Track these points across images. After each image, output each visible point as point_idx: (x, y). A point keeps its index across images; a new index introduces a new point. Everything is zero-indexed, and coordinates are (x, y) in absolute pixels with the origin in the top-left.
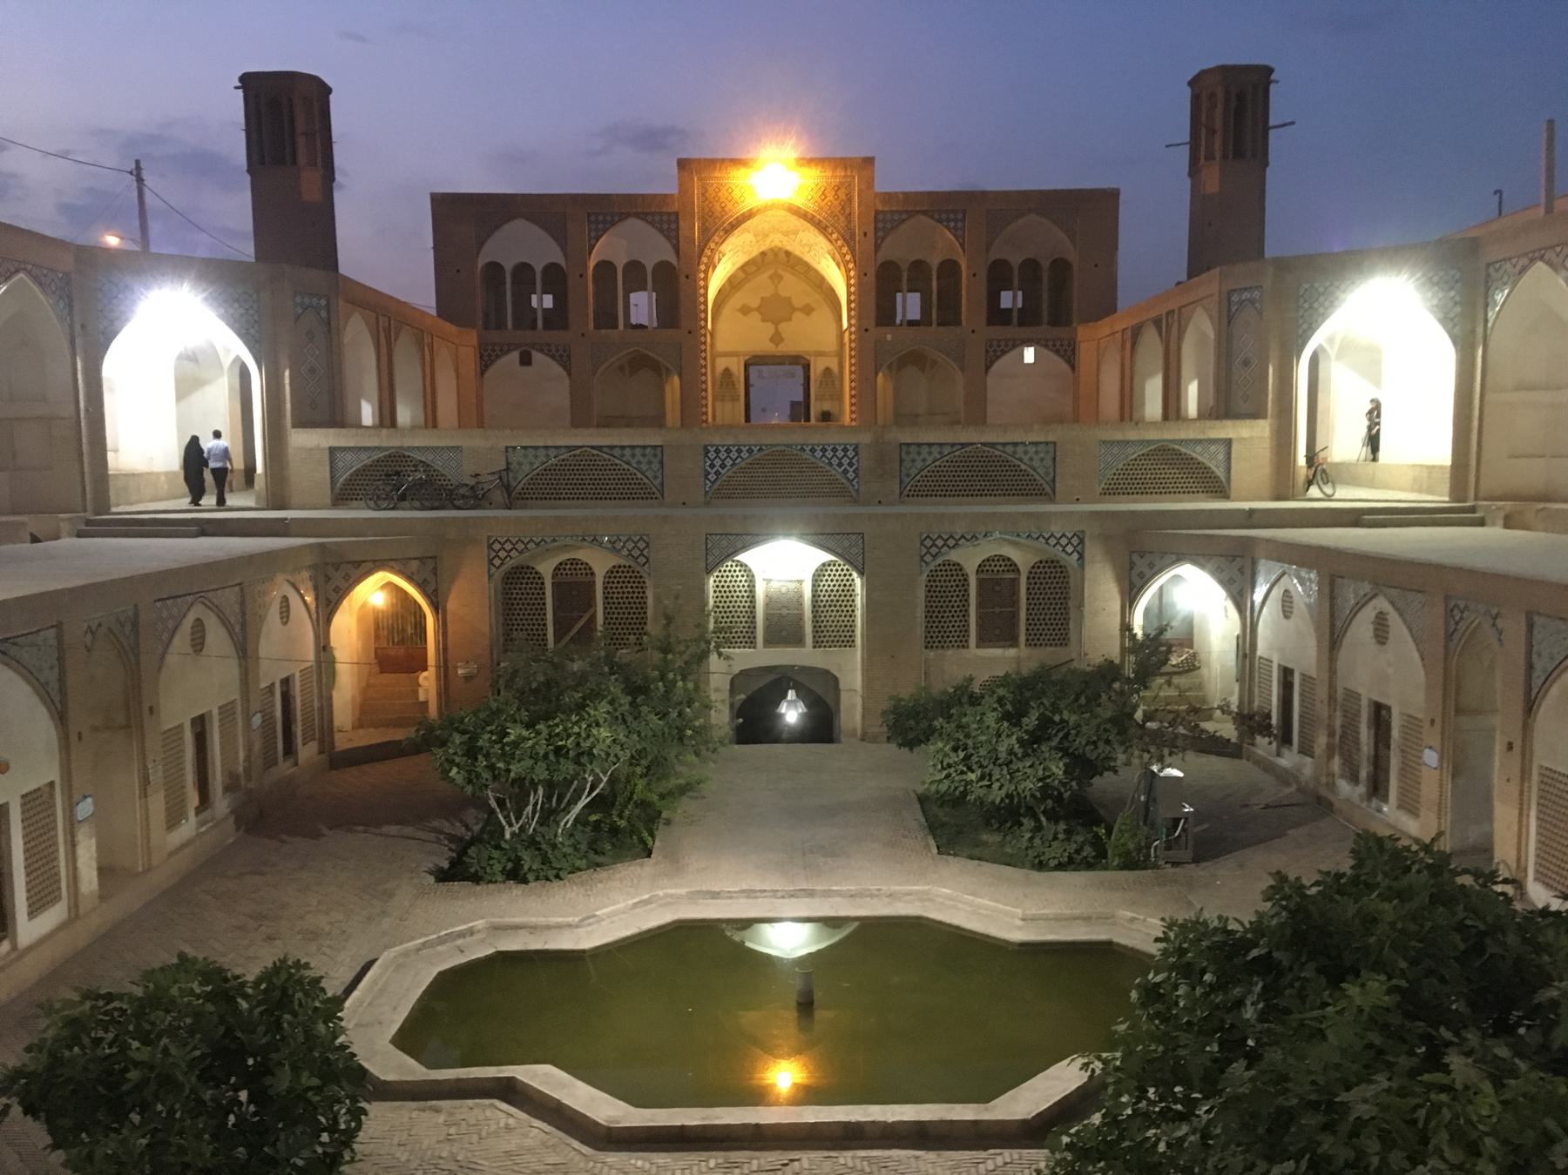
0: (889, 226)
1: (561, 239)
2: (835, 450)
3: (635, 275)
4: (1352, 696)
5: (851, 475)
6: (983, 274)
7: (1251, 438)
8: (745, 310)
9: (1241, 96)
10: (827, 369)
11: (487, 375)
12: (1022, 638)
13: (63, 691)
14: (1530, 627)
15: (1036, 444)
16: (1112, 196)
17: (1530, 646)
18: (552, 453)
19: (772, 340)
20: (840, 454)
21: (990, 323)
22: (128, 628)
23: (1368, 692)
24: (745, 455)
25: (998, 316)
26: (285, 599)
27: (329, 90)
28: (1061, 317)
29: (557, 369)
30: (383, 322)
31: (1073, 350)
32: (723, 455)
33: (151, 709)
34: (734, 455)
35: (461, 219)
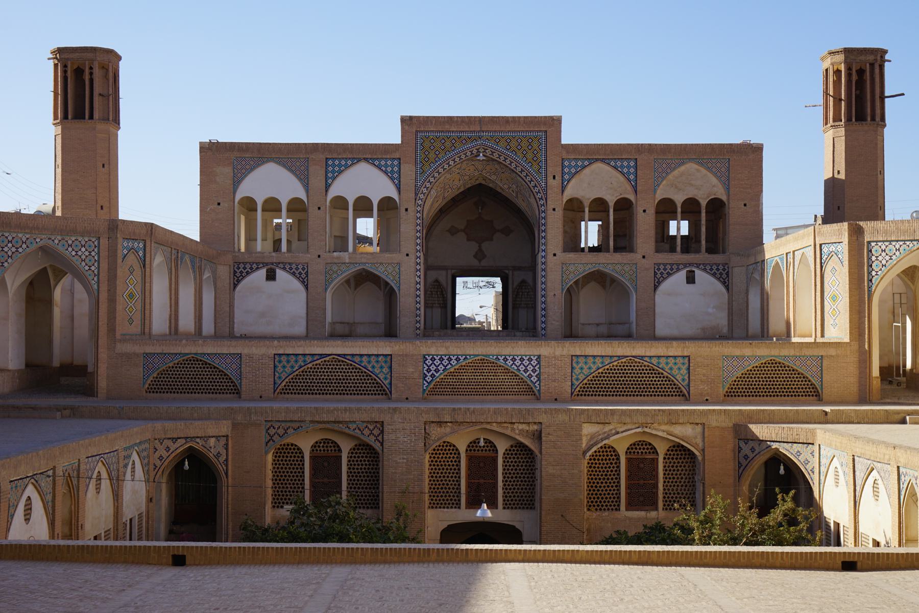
0: (573, 170)
1: (305, 181)
2: (522, 360)
3: (363, 207)
5: (534, 379)
6: (651, 211)
7: (838, 356)
8: (453, 231)
9: (861, 72)
10: (523, 281)
11: (238, 289)
12: (660, 504)
13: (54, 511)
15: (675, 357)
16: (757, 150)
18: (309, 359)
19: (475, 256)
20: (526, 362)
21: (658, 251)
24: (454, 362)
25: (665, 241)
26: (134, 464)
27: (120, 58)
29: (296, 284)
31: (727, 274)
32: (437, 362)
34: (445, 362)
35: (224, 163)
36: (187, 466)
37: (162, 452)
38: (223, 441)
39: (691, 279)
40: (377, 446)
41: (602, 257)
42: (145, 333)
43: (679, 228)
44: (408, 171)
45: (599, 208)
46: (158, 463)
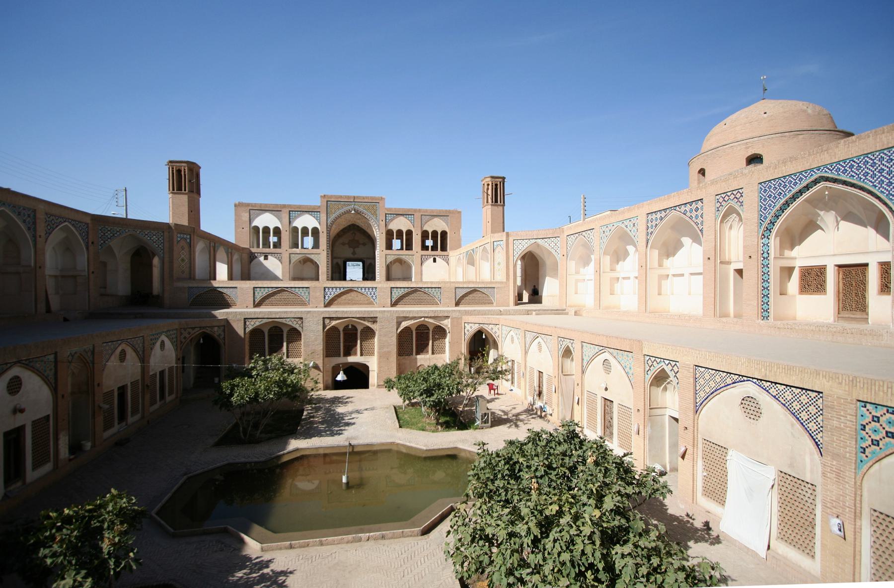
3: (305, 231)
4: (532, 368)
8: (343, 244)
9: (496, 185)
14: (582, 346)
17: (582, 353)
21: (422, 249)
22: (89, 354)
23: (537, 368)
26: (163, 342)
28: (444, 248)
30: (212, 244)
33: (98, 385)
36: (202, 341)
37: (185, 334)
38: (222, 328)
39: (435, 261)
40: (300, 329)
41: (401, 252)
42: (191, 277)
43: (429, 243)
44: (323, 216)
45: (400, 233)
46: (183, 340)
